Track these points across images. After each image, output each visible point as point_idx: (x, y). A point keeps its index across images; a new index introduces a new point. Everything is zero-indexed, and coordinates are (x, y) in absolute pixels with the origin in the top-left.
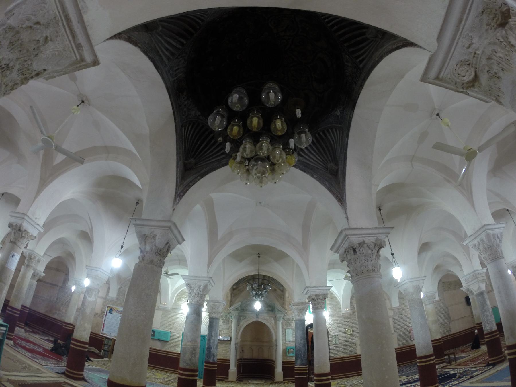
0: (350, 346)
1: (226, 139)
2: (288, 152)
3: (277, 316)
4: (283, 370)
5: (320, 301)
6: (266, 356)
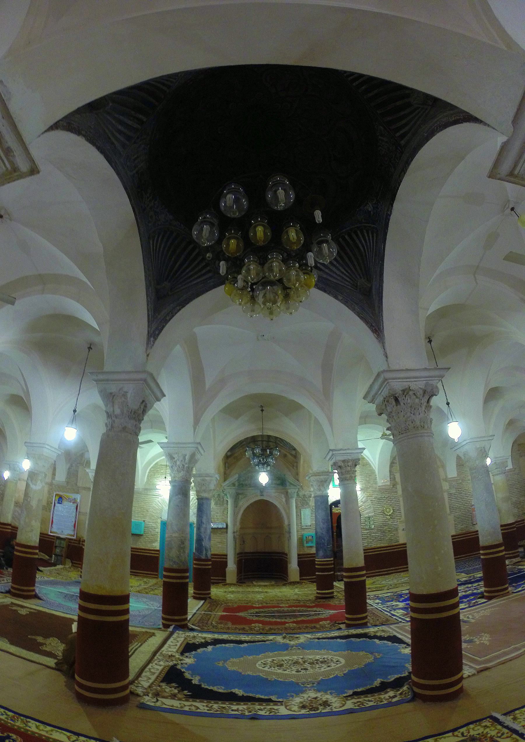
0: (389, 531)
1: (219, 256)
2: (305, 269)
3: (289, 491)
4: (299, 565)
5: (349, 468)
6: (275, 548)
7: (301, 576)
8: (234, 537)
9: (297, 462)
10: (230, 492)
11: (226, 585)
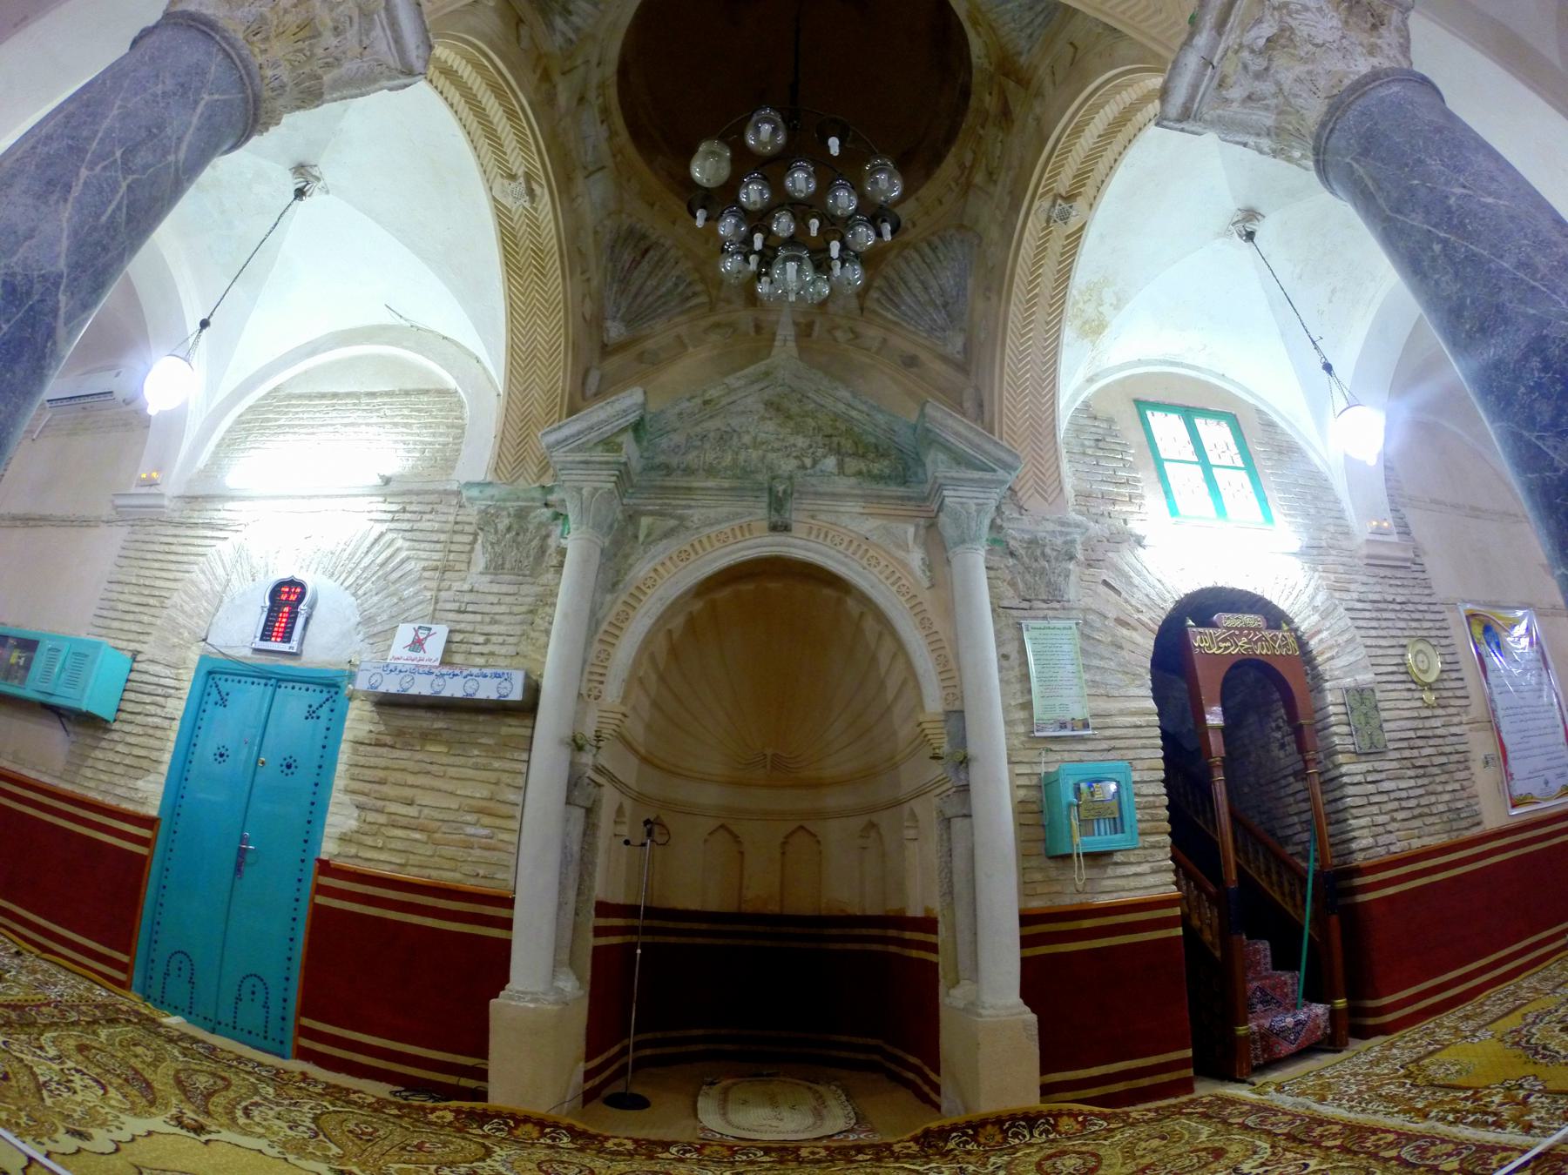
4: (1029, 993)
9: (977, 389)
10: (585, 488)
11: (483, 1118)
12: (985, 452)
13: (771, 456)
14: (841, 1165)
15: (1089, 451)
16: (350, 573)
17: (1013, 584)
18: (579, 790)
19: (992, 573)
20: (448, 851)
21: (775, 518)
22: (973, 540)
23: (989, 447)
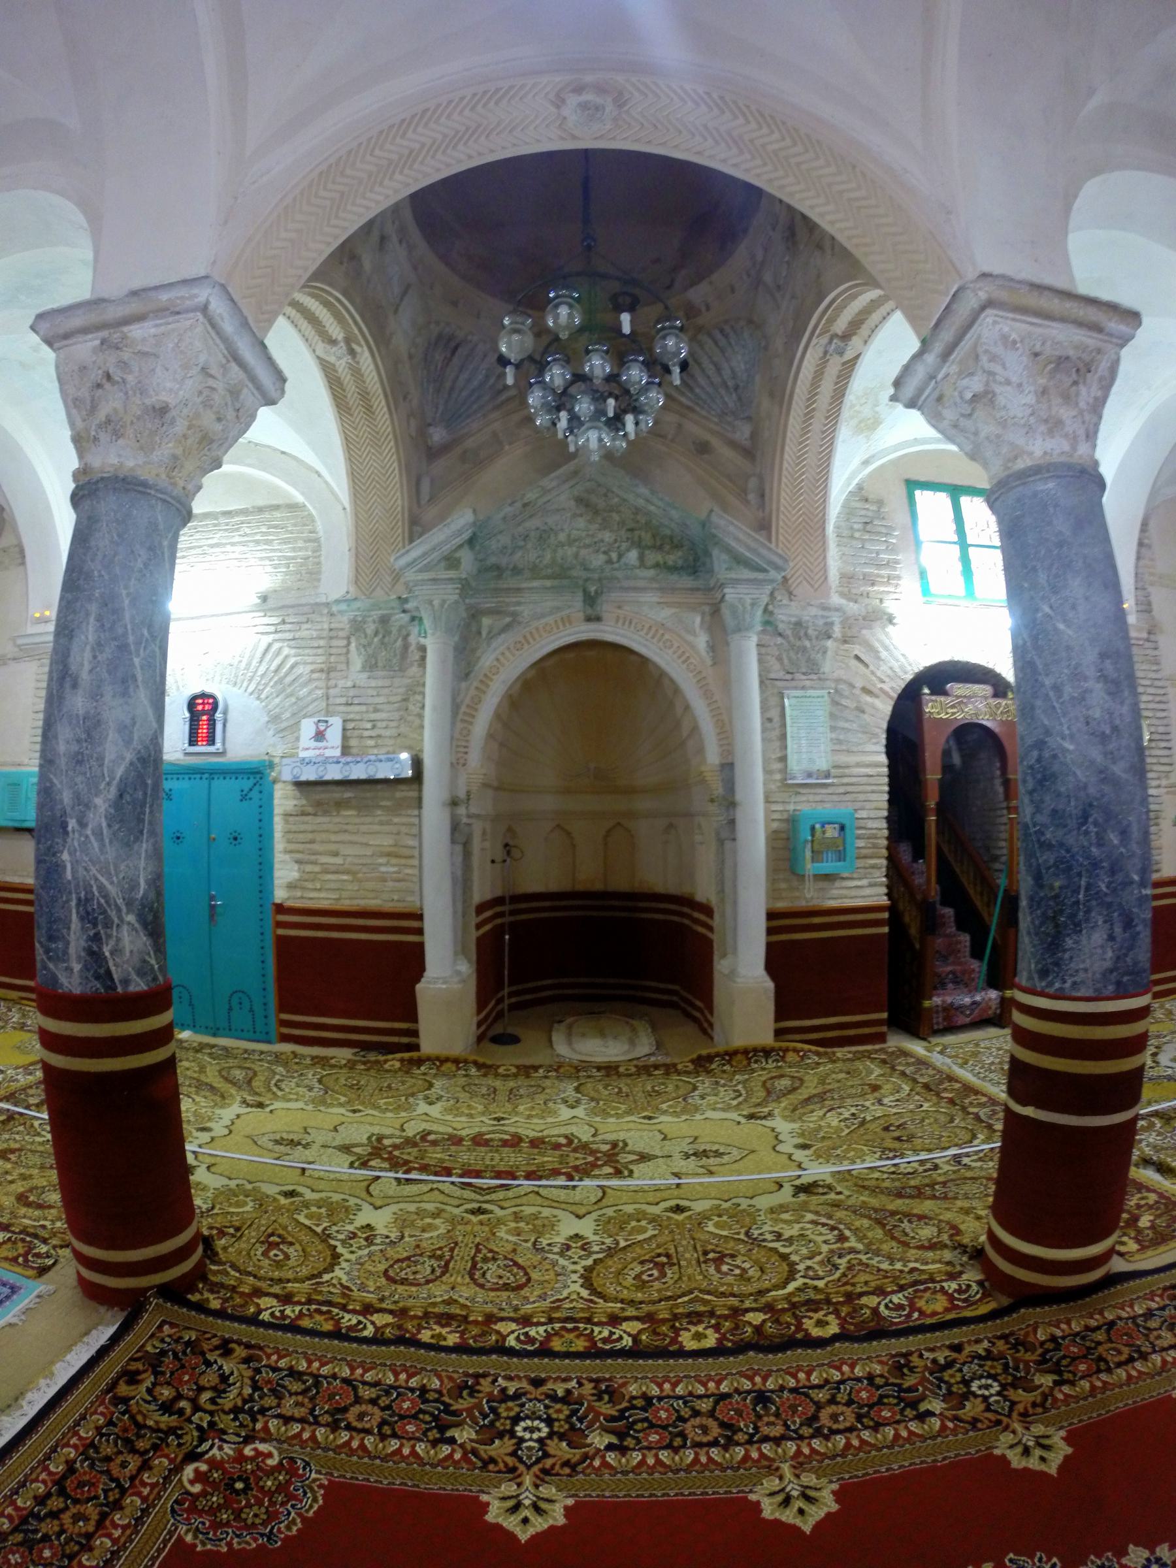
3: (730, 593)
4: (772, 966)
7: (780, 1015)
8: (455, 827)
9: (761, 478)
12: (759, 555)
13: (583, 552)
14: (644, 1077)
15: (857, 535)
16: (250, 681)
17: (779, 659)
18: (458, 832)
19: (763, 650)
20: (370, 885)
21: (589, 611)
22: (747, 629)
23: (764, 552)
